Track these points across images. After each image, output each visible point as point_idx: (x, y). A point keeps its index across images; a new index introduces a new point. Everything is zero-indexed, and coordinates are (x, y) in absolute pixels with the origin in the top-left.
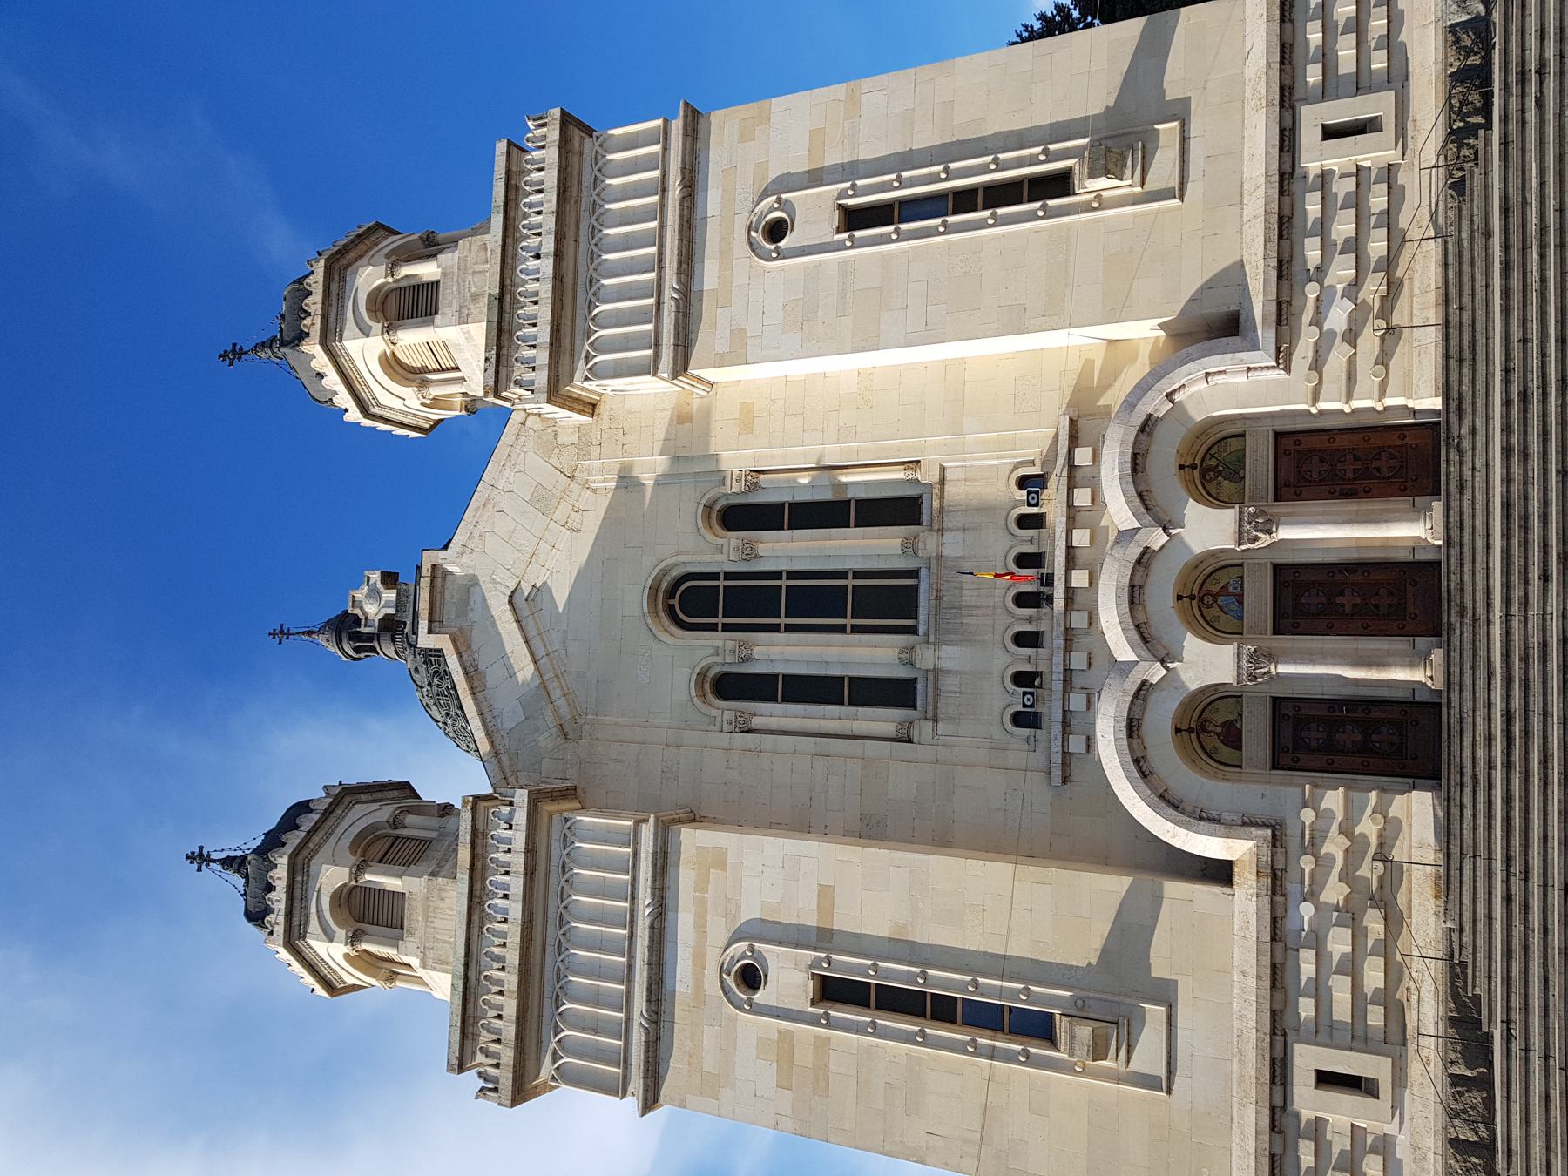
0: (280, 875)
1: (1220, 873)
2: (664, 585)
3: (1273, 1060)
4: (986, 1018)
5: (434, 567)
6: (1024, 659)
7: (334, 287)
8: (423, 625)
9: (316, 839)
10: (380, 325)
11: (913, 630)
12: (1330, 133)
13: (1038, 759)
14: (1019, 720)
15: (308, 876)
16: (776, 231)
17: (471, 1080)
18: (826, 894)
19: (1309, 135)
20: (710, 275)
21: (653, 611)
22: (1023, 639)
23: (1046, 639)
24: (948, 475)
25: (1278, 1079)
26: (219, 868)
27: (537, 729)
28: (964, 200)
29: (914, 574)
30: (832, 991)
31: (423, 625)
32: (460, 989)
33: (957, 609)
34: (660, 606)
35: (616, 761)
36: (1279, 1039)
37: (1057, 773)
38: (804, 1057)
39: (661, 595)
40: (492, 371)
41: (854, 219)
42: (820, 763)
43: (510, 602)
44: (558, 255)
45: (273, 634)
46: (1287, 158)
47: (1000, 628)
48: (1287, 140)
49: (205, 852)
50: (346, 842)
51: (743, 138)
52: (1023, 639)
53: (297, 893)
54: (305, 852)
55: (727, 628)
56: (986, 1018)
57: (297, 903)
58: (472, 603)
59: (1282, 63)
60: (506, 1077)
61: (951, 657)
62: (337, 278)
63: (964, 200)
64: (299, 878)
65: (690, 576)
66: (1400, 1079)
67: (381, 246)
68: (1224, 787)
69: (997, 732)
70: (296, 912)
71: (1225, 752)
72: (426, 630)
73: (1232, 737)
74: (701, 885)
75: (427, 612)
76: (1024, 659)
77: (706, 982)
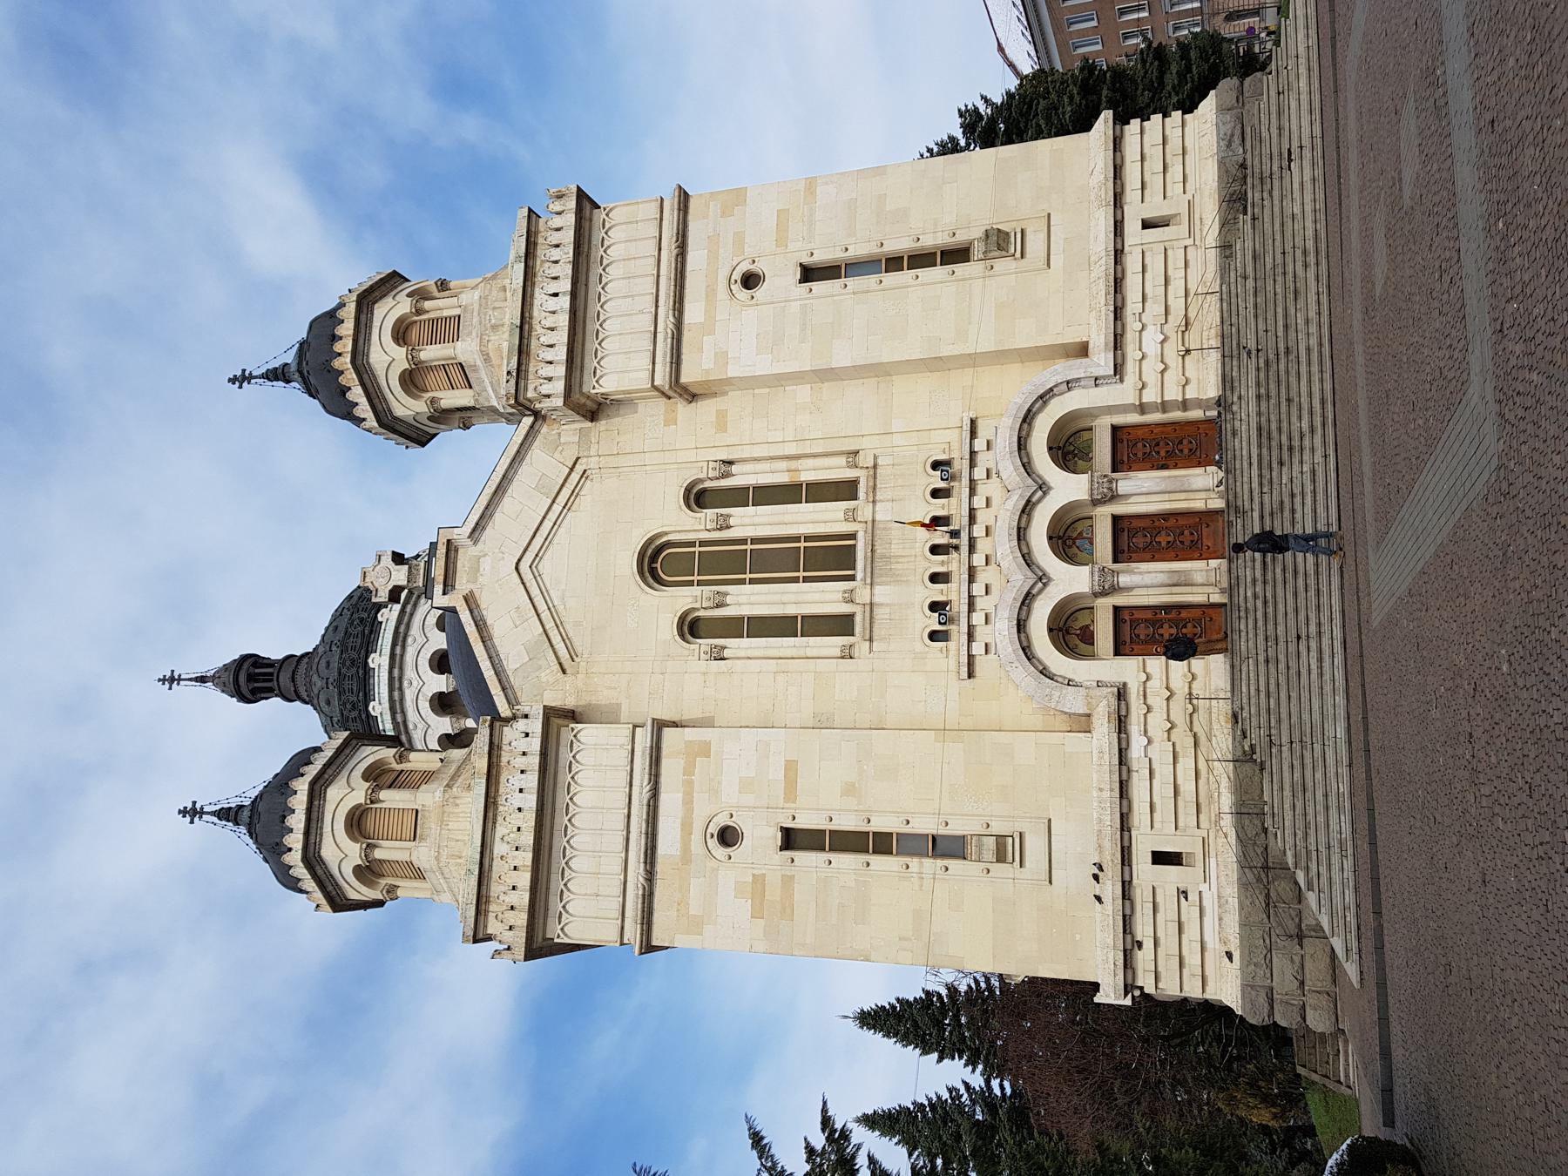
0: (299, 802)
2: (650, 551)
3: (1122, 848)
5: (448, 541)
6: (937, 592)
7: (363, 317)
8: (438, 589)
9: (330, 771)
10: (405, 349)
11: (852, 578)
12: (1147, 225)
14: (933, 636)
15: (325, 800)
16: (750, 281)
19: (1132, 227)
20: (694, 313)
21: (641, 573)
22: (935, 578)
23: (955, 577)
24: (880, 462)
25: (1126, 863)
26: (215, 819)
27: (540, 667)
29: (853, 536)
30: (791, 839)
32: (476, 872)
33: (888, 558)
34: (646, 568)
35: (610, 688)
36: (1126, 833)
38: (774, 892)
39: (646, 560)
41: (809, 274)
42: (780, 677)
43: (517, 569)
44: (574, 295)
45: (163, 680)
46: (1119, 240)
47: (921, 570)
48: (1118, 228)
49: (198, 806)
51: (723, 215)
52: (935, 578)
53: (314, 815)
54: (322, 781)
55: (700, 583)
57: (314, 825)
58: (481, 569)
59: (1115, 178)
60: (519, 939)
61: (882, 593)
62: (365, 311)
63: (894, 263)
64: (316, 803)
65: (669, 544)
67: (400, 288)
69: (919, 647)
70: (313, 831)
72: (441, 592)
73: (1088, 637)
74: (689, 770)
75: (442, 578)
76: (937, 592)
77: (692, 843)
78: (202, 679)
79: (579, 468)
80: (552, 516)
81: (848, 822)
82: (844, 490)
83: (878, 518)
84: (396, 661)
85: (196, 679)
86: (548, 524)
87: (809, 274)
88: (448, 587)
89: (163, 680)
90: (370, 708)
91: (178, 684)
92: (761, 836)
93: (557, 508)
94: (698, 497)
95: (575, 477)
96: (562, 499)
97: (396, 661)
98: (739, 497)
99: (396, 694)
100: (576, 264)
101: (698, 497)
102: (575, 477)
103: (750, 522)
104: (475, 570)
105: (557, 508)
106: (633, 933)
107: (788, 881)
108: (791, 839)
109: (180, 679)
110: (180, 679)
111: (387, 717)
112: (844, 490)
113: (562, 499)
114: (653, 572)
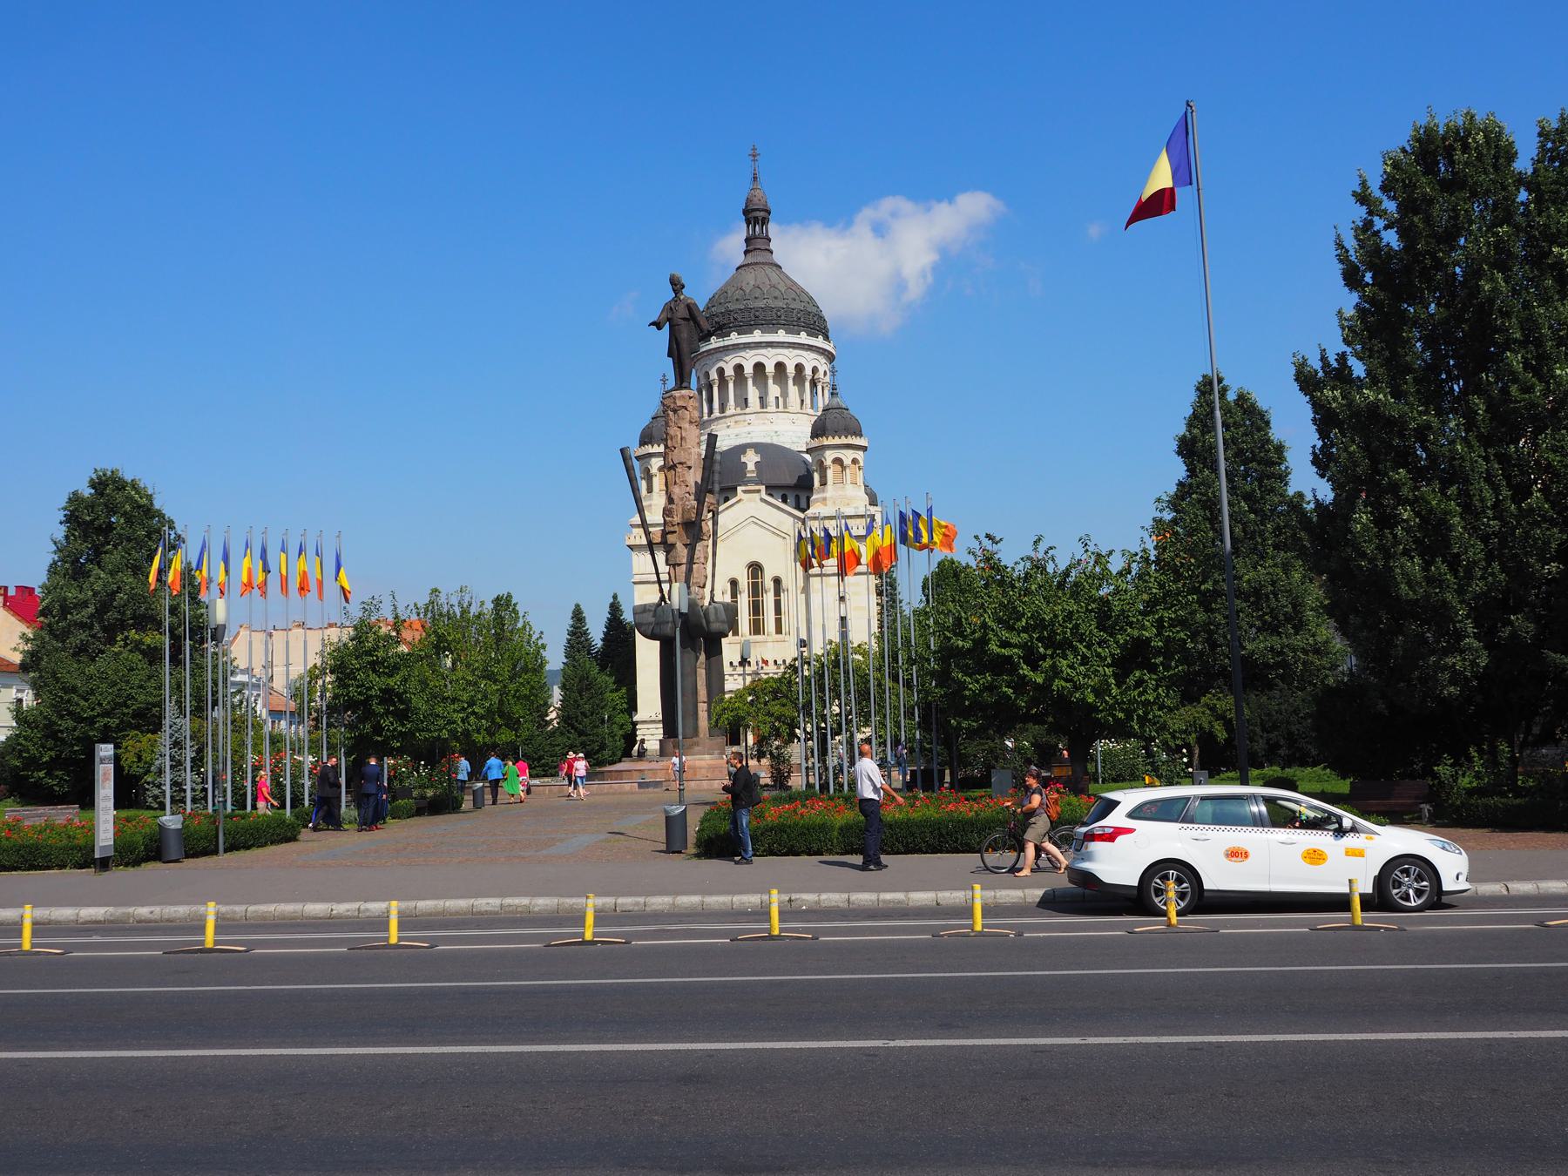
11: (750, 634)
29: (764, 634)
31: (744, 488)
45: (754, 149)
79: (786, 536)
80: (770, 528)
82: (779, 630)
83: (769, 644)
84: (758, 345)
86: (766, 526)
88: (745, 492)
89: (754, 149)
93: (773, 529)
94: (777, 581)
95: (783, 535)
96: (775, 531)
97: (758, 345)
98: (777, 593)
99: (742, 346)
101: (777, 581)
102: (783, 535)
103: (769, 600)
104: (750, 500)
105: (773, 529)
106: (637, 578)
109: (754, 160)
112: (779, 630)
113: (775, 531)
114: (756, 565)
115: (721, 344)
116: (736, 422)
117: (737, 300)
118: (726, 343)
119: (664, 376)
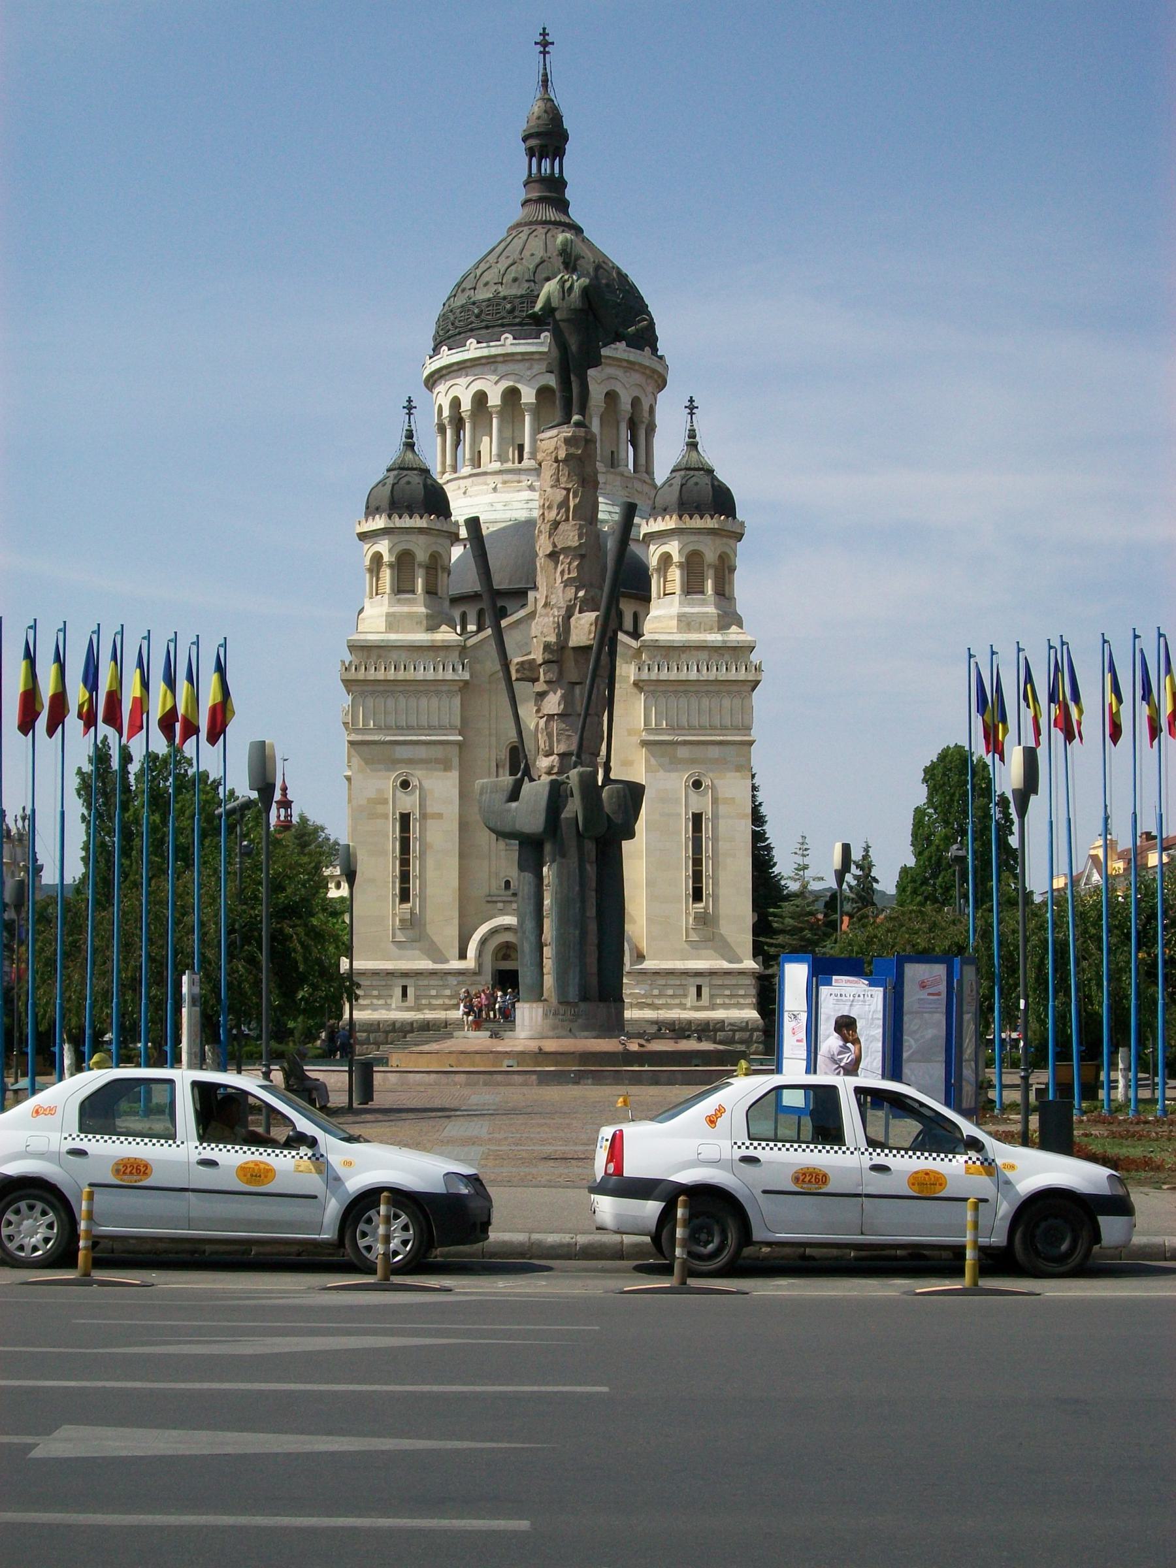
1: (463, 956)
4: (405, 877)
13: (494, 891)
17: (348, 657)
18: (439, 816)
28: (697, 862)
30: (405, 819)
37: (489, 899)
38: (380, 809)
40: (651, 644)
50: (434, 548)
56: (405, 877)
60: (352, 675)
63: (697, 862)
66: (409, 1009)
68: (490, 957)
69: (502, 875)
71: (500, 955)
73: (506, 957)
78: (545, 82)
81: (415, 847)
85: (545, 75)
87: (697, 819)
90: (507, 335)
91: (541, 52)
92: (409, 802)
99: (520, 357)
100: (717, 681)
107: (386, 816)
108: (405, 819)
109: (544, 53)
110: (544, 53)
111: (500, 351)
115: (485, 352)
116: (505, 482)
117: (515, 280)
118: (494, 351)
119: (410, 401)
